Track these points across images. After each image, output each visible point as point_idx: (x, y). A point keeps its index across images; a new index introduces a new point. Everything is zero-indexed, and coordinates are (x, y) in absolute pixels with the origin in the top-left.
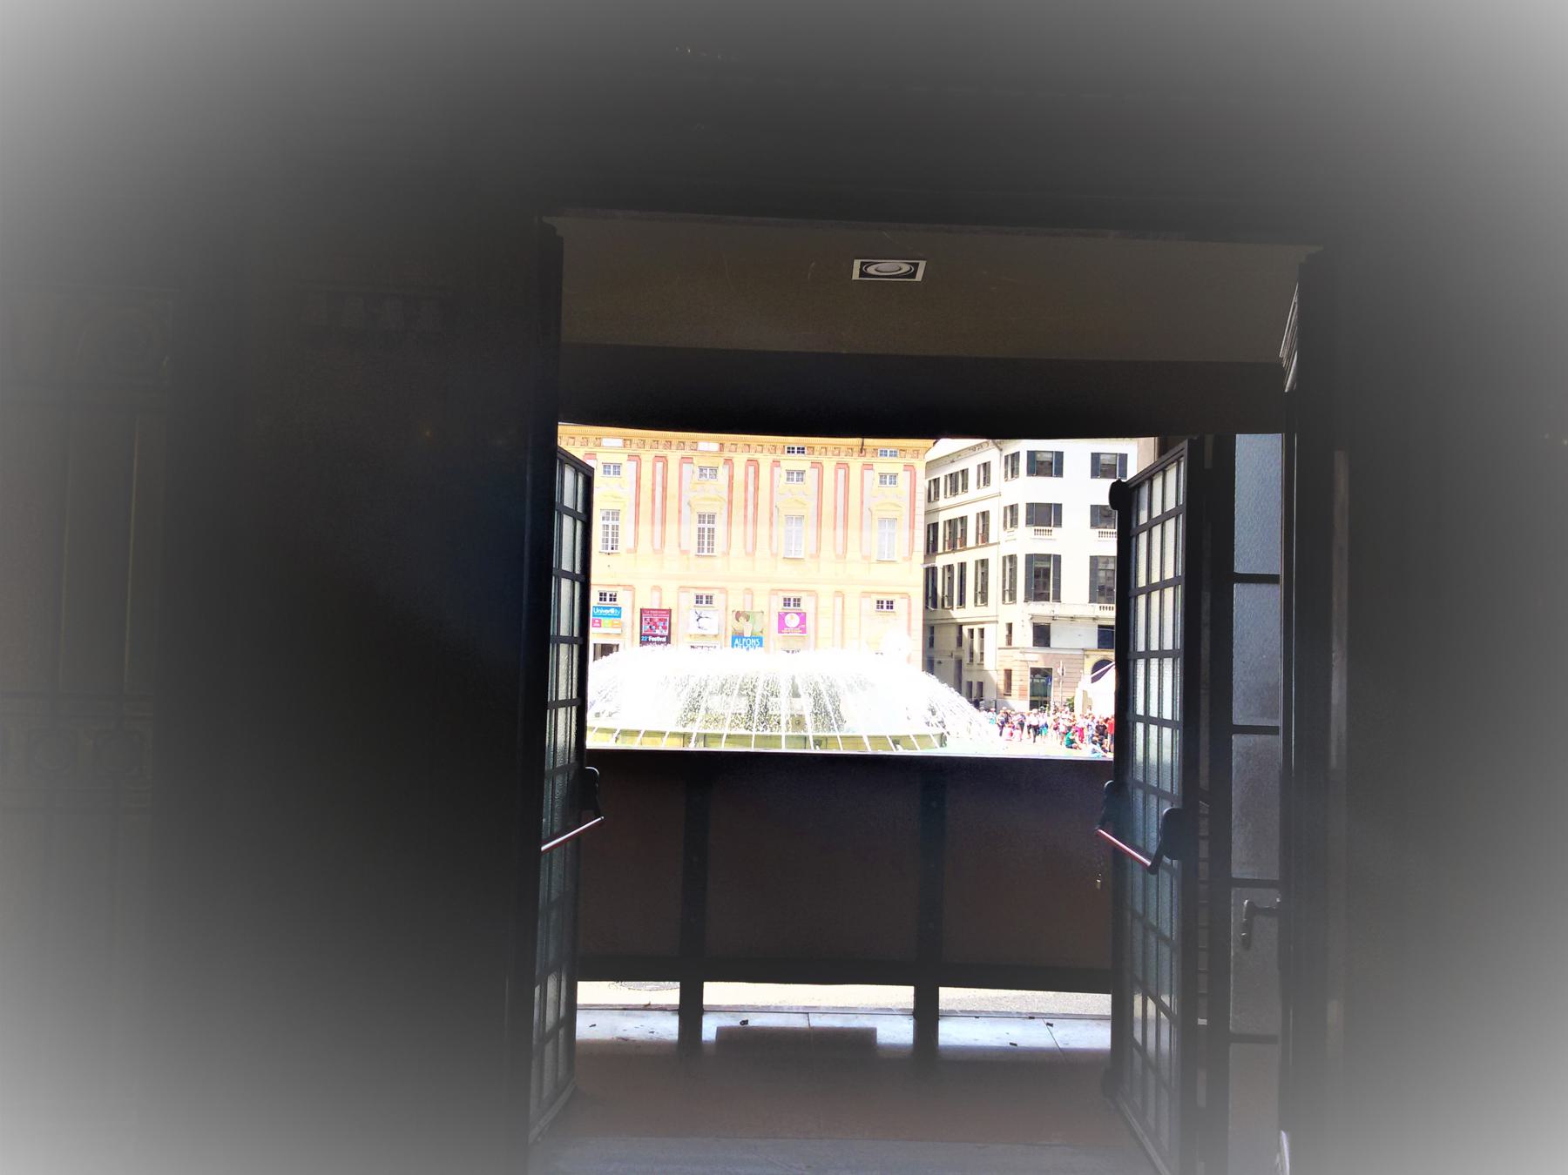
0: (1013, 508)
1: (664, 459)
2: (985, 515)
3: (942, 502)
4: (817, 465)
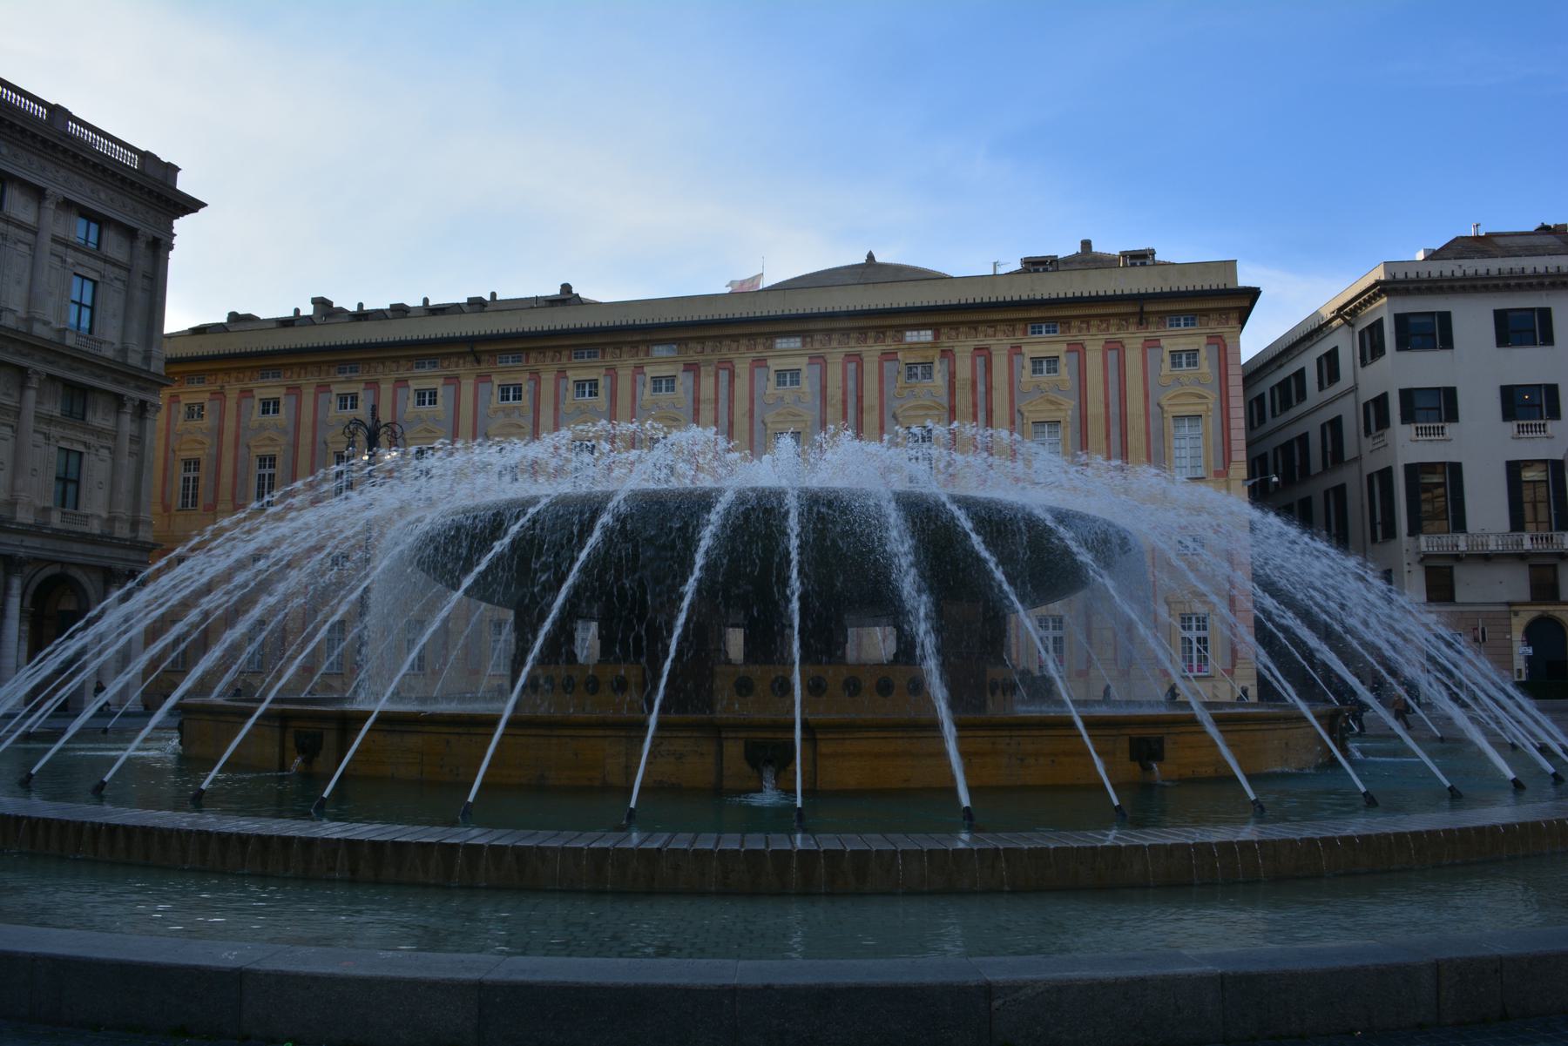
0: (1381, 402)
1: (858, 359)
2: (1336, 423)
3: (1271, 423)
4: (1077, 349)
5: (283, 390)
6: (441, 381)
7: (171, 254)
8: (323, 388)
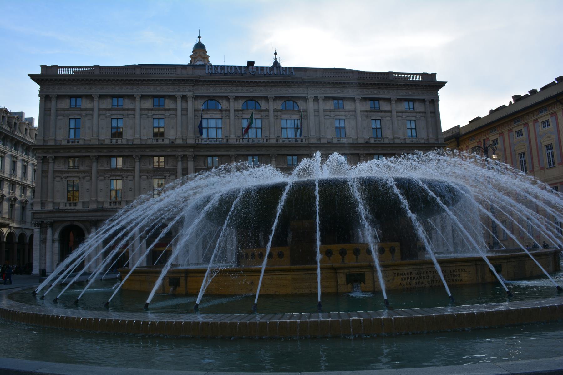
5: (498, 135)
6: (550, 116)
7: (439, 102)
8: (510, 131)
